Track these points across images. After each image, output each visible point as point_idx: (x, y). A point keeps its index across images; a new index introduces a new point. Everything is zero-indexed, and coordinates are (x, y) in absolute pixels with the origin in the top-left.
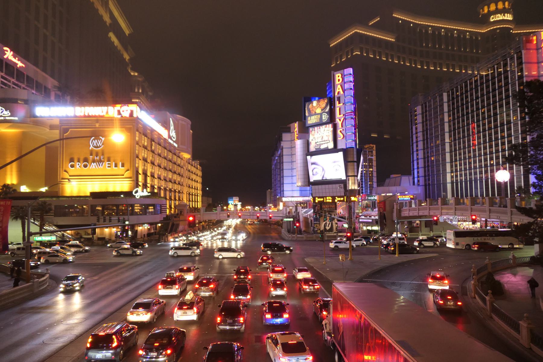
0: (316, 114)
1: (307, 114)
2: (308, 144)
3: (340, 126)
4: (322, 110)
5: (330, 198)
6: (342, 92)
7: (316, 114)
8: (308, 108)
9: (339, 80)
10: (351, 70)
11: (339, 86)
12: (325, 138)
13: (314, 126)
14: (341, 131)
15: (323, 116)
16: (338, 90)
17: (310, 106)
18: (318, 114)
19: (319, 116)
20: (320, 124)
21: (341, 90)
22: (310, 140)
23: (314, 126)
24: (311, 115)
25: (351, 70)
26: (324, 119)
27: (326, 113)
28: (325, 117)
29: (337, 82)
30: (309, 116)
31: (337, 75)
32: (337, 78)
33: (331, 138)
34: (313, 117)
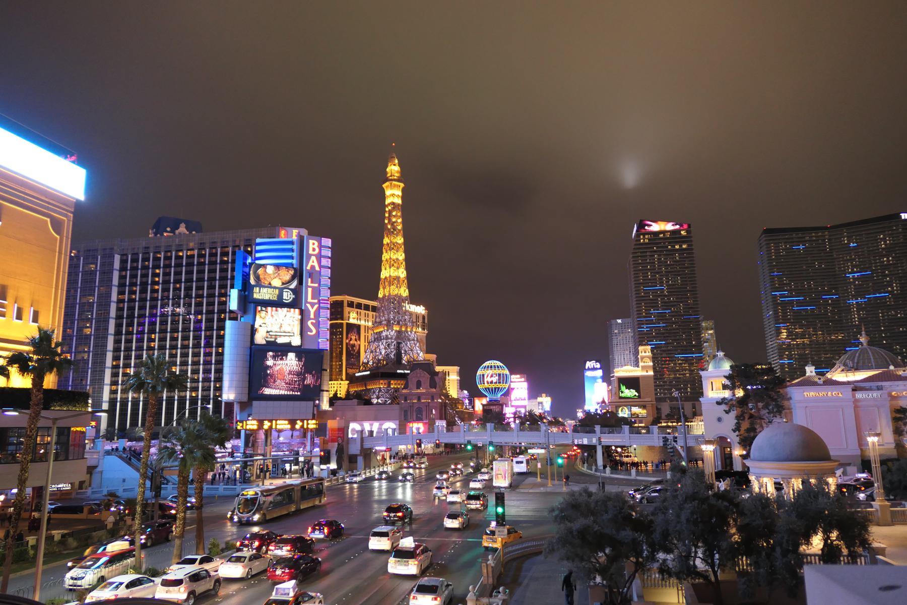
0: (270, 286)
1: (252, 282)
2: (253, 331)
3: (312, 316)
4: (283, 284)
5: (255, 422)
6: (317, 268)
7: (270, 286)
8: (255, 273)
9: (314, 250)
10: (327, 242)
11: (313, 258)
12: (286, 328)
13: (266, 304)
14: (312, 323)
15: (285, 294)
16: (310, 263)
17: (260, 271)
18: (275, 288)
19: (277, 291)
20: (278, 304)
21: (316, 264)
22: (256, 326)
23: (266, 304)
24: (259, 284)
25: (327, 242)
26: (285, 297)
27: (291, 290)
28: (288, 296)
29: (311, 252)
30: (256, 286)
31: (311, 242)
32: (311, 247)
33: (297, 329)
34: (264, 290)
